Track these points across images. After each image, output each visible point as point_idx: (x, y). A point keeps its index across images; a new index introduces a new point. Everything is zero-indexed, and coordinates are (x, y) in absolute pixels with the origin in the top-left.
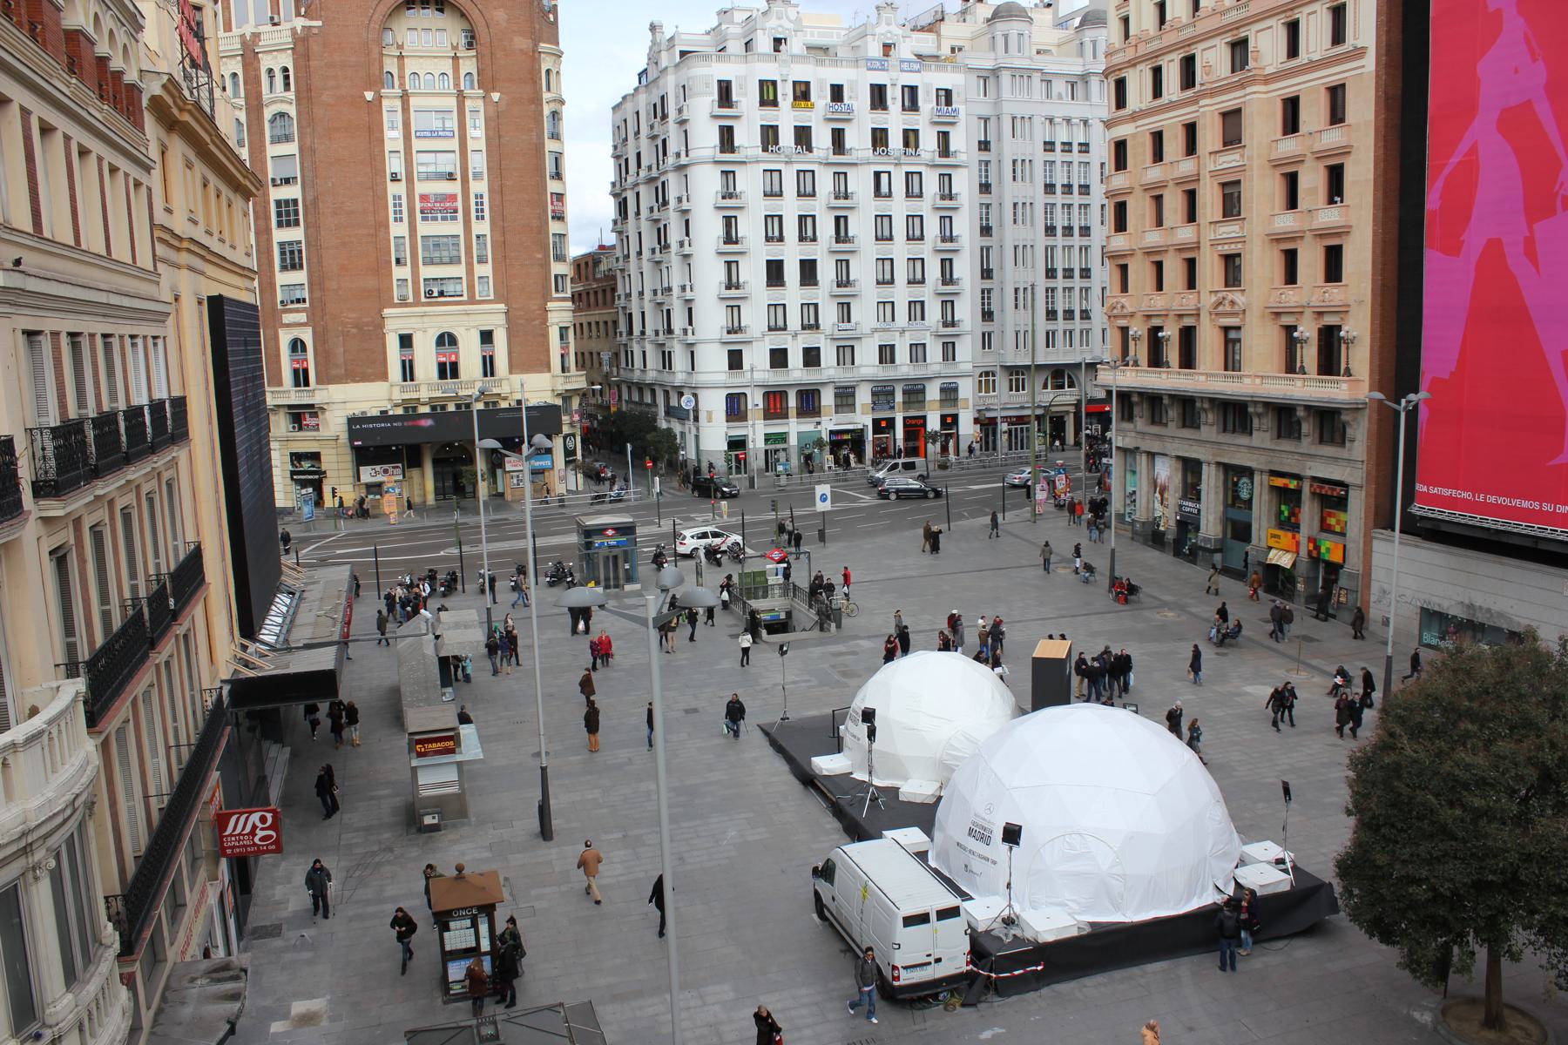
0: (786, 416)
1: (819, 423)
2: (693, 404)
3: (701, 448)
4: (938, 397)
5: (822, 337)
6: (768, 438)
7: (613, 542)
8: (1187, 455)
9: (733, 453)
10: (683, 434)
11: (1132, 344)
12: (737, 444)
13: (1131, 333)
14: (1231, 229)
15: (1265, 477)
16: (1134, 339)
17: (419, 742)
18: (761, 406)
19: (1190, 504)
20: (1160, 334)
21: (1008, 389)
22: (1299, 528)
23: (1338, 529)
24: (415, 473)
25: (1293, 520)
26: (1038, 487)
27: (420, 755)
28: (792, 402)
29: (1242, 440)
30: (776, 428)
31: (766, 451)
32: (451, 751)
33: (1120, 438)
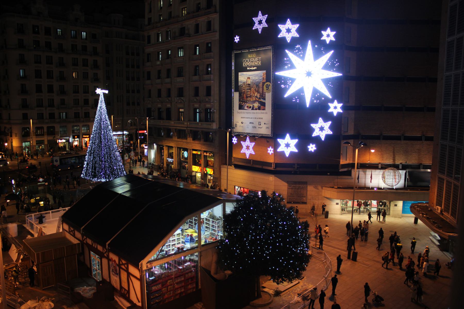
0: (42, 135)
2: (10, 131)
8: (169, 145)
11: (152, 113)
13: (152, 110)
14: (180, 79)
15: (191, 151)
18: (34, 132)
19: (170, 159)
20: (160, 110)
22: (201, 165)
23: (212, 165)
25: (199, 163)
26: (125, 156)
28: (45, 130)
29: (185, 141)
30: (40, 139)
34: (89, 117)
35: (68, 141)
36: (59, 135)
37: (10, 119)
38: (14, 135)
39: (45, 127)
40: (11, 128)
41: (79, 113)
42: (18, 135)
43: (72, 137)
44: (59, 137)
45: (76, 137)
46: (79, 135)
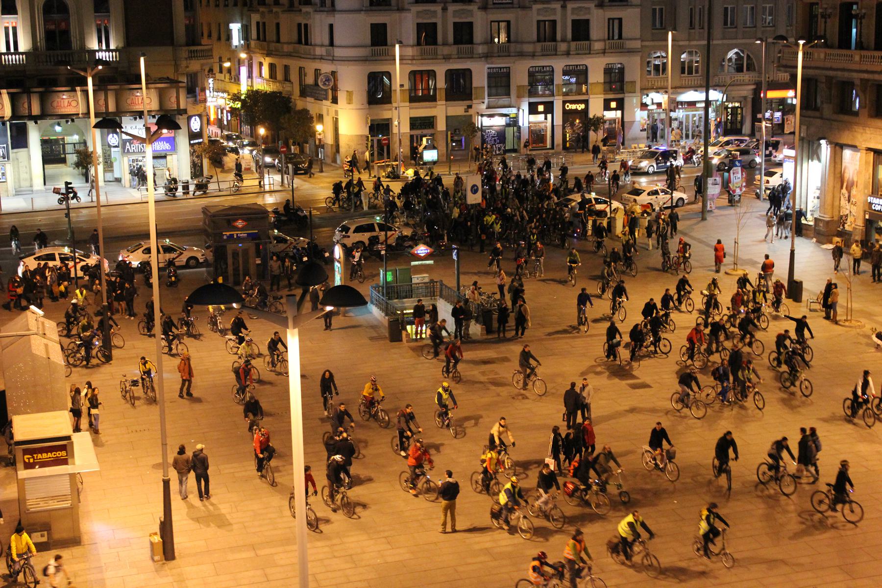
0: (433, 99)
1: (470, 107)
2: (332, 84)
3: (342, 131)
4: (601, 79)
5: (473, 7)
6: (416, 123)
7: (243, 234)
9: (375, 139)
10: (320, 118)
12: (379, 128)
16: (824, 16)
17: (26, 452)
18: (406, 87)
21: (679, 71)
24: (22, 152)
26: (710, 181)
27: (29, 466)
28: (441, 83)
30: (422, 111)
31: (412, 137)
32: (64, 462)
33: (804, 128)
34: (587, 37)
35: (514, 122)
36: (486, 101)
37: (332, 44)
38: (342, 97)
39: (441, 70)
40: (333, 73)
41: (554, 22)
42: (355, 98)
43: (525, 107)
44: (484, 106)
45: (541, 108)
46: (552, 103)
